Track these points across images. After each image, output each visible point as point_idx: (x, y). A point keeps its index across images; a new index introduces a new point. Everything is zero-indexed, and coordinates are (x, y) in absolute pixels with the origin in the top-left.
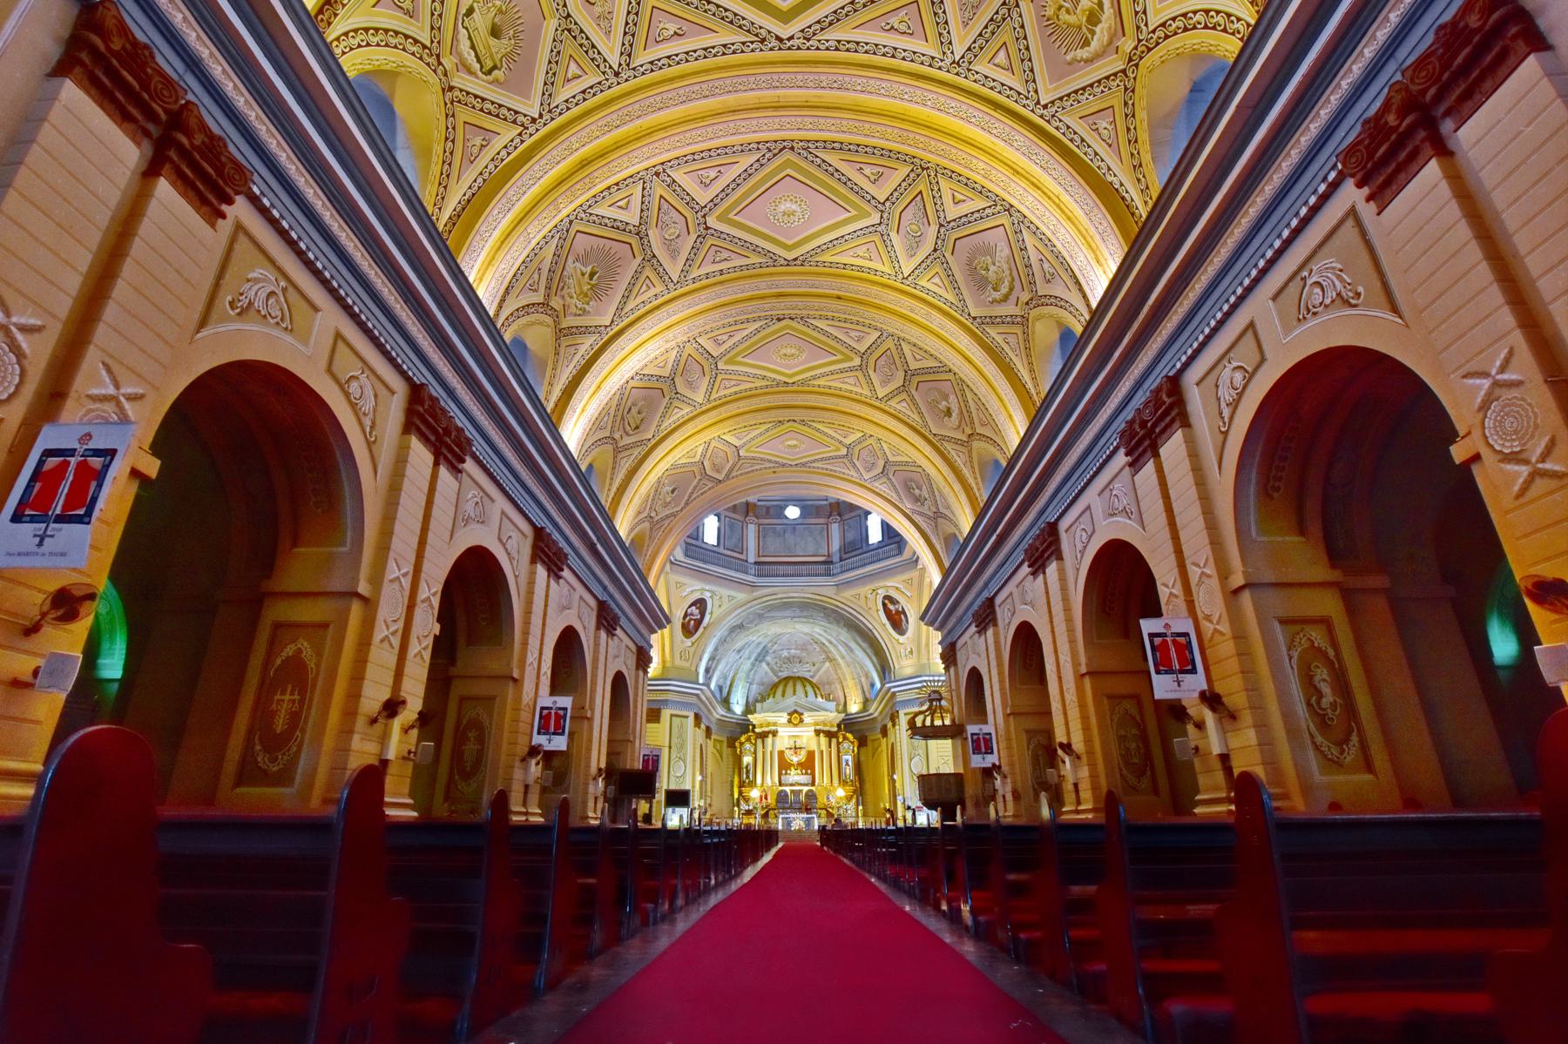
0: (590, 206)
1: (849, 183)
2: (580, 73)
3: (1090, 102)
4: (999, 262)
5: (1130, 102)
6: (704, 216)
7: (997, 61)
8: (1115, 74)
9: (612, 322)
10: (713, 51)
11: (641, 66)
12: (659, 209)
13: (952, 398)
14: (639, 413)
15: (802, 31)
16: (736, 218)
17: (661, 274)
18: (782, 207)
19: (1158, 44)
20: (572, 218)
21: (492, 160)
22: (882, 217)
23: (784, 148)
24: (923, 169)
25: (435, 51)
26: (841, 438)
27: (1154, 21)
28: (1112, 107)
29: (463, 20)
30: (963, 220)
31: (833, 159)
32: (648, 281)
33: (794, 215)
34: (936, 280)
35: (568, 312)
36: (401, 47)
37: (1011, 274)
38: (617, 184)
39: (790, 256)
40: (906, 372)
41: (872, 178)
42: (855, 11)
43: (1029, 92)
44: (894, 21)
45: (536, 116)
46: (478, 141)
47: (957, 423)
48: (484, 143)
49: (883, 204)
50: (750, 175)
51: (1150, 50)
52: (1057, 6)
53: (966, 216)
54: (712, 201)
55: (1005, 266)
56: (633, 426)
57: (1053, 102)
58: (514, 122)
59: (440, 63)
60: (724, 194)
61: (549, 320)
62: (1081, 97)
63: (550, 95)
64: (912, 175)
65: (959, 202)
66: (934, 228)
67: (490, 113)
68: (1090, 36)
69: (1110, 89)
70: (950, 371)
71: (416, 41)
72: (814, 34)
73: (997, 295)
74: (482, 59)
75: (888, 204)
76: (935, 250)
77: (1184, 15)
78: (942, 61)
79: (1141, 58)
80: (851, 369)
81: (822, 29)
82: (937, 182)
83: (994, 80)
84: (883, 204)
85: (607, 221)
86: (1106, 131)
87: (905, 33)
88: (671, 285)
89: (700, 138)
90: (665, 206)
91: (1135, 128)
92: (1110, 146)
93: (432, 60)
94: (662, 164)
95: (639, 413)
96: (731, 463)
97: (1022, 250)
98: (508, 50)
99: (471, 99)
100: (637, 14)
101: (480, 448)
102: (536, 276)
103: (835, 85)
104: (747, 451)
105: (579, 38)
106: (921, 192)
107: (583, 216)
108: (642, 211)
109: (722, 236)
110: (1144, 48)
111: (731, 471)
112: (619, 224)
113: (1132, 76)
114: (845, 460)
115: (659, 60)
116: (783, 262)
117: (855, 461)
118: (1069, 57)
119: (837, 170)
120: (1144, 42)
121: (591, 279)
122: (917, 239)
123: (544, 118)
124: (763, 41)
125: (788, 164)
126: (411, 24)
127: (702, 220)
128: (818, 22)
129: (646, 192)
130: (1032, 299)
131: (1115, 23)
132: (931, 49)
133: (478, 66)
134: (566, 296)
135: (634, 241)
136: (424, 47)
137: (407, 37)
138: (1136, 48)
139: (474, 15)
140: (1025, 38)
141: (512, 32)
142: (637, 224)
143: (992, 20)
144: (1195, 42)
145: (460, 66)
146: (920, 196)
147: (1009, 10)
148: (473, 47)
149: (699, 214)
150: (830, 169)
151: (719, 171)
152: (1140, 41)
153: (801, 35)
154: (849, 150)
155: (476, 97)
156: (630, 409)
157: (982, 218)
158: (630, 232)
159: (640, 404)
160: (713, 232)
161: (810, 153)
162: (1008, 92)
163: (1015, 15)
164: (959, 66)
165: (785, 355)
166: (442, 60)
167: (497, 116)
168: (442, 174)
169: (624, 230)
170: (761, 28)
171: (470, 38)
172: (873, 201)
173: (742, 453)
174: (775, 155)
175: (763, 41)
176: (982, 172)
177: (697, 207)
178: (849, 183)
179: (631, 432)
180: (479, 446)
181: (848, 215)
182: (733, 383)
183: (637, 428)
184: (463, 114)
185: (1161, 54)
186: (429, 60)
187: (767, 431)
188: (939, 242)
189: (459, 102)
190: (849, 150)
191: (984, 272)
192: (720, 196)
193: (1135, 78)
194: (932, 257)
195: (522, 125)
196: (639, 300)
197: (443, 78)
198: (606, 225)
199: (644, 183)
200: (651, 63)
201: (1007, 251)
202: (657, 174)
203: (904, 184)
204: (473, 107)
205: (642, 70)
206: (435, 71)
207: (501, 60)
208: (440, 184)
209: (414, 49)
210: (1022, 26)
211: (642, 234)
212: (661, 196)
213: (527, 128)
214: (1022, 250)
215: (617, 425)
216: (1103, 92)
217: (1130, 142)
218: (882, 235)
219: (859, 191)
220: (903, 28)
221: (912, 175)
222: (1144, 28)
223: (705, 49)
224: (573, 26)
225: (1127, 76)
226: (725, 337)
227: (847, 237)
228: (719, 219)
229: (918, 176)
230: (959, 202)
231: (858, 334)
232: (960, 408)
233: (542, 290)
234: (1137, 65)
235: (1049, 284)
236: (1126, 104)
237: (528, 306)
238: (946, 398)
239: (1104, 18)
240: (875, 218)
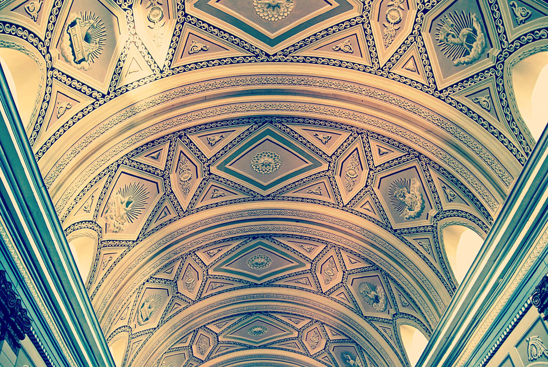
0: (133, 156)
1: (308, 144)
2: (138, 68)
3: (461, 92)
4: (412, 191)
5: (501, 84)
6: (209, 166)
7: (407, 66)
9: (138, 238)
10: (225, 61)
11: (178, 68)
12: (179, 160)
13: (379, 288)
14: (149, 308)
15: (283, 51)
16: (231, 167)
17: (175, 205)
18: (262, 161)
19: (516, 50)
20: (120, 162)
21: (72, 118)
22: (329, 166)
23: (266, 122)
24: (358, 134)
25: (47, 44)
26: (294, 325)
27: (511, 38)
28: (489, 88)
29: (68, 29)
30: (386, 165)
31: (298, 129)
32: (166, 210)
33: (270, 166)
34: (367, 206)
35: (108, 229)
36: (25, 38)
37: (422, 199)
38: (153, 142)
39: (265, 193)
40: (344, 272)
41: (324, 141)
42: (317, 40)
43: (430, 83)
44: (341, 45)
45: (106, 93)
46: (65, 105)
47: (383, 307)
48: (69, 107)
49: (331, 157)
50: (242, 139)
51: (510, 53)
52: (446, 34)
53: (388, 162)
54: (215, 155)
55: (417, 194)
56: (145, 318)
57: (446, 89)
58: (91, 95)
59: (48, 52)
60: (223, 151)
61: (95, 234)
62: (466, 84)
63: (117, 81)
64: (351, 138)
65: (384, 153)
66: (366, 171)
67: (75, 88)
68: (469, 49)
69: (485, 78)
70: (377, 269)
71: (36, 36)
72: (290, 53)
73: (412, 213)
74: (76, 53)
75: (334, 157)
76: (366, 186)
77: (533, 32)
78: (371, 68)
79: (505, 59)
80: (304, 272)
81: (295, 50)
82: (368, 142)
83: (406, 78)
84: (331, 157)
85: (143, 166)
86: (485, 103)
87: (348, 52)
88: (182, 213)
89: (212, 114)
90: (183, 158)
91: (506, 99)
92: (489, 111)
93: (44, 49)
94: (184, 130)
95: (149, 308)
96: (212, 346)
97: (429, 182)
98: (94, 50)
99: (64, 78)
100: (179, 36)
101: (35, 328)
102: (90, 201)
103: (302, 83)
104: (224, 337)
105: (140, 49)
106: (357, 149)
107: (127, 162)
108: (167, 161)
109: (220, 179)
110: (507, 53)
111: (211, 353)
112: (151, 169)
113: (500, 69)
114: (296, 341)
115: (190, 65)
116: (260, 197)
117: (304, 341)
118: (455, 62)
119: (300, 136)
120: (506, 50)
121: (127, 207)
122: (354, 180)
123: (110, 95)
124: (257, 56)
125: (268, 132)
126: (35, 26)
127: (207, 168)
128: (293, 46)
129: (171, 149)
130: (438, 214)
131: (486, 41)
132: (365, 61)
133: (73, 57)
134: (109, 217)
135: (160, 181)
136: (40, 40)
137: (30, 32)
138: (501, 53)
139: (76, 26)
140: (426, 53)
141: (98, 40)
142: (163, 170)
143: (404, 43)
144: (542, 46)
145: (61, 56)
146: (356, 151)
147: (415, 37)
148: (71, 46)
149: (206, 164)
150: (296, 135)
152: (503, 49)
153: (281, 53)
154: (309, 123)
155: (68, 76)
156: (144, 304)
157: (399, 163)
158: (158, 175)
159: (150, 302)
160: (214, 176)
161: (283, 125)
162: (416, 85)
163: (419, 40)
164: (383, 71)
165: (257, 263)
166: (49, 50)
167: (80, 90)
168: (37, 123)
169: (154, 173)
170: (256, 48)
171: (70, 40)
172: (323, 156)
173: (220, 339)
174: (259, 126)
175: (257, 56)
176: (400, 133)
177: (204, 159)
178: (308, 144)
179: (142, 323)
180: (36, 327)
181: (307, 165)
182: (218, 285)
183: (147, 319)
184: (57, 86)
185: (519, 55)
186: (41, 49)
187: (240, 321)
188: (369, 181)
189: (56, 78)
190: (309, 123)
191: (401, 199)
192: (221, 153)
193: (502, 70)
194: (364, 191)
195: (96, 98)
196: (159, 222)
197: (49, 62)
198: (142, 169)
199: (171, 142)
200: (185, 66)
201: (418, 184)
202: (180, 137)
203: (345, 144)
204: (65, 83)
205: (178, 70)
206: (44, 56)
208: (34, 129)
209: (34, 40)
210: (424, 46)
211: (165, 177)
212: (181, 152)
213: (98, 100)
214: (429, 182)
215: (133, 316)
216: (480, 80)
217: (503, 107)
218: (329, 178)
219: (316, 151)
220: (347, 49)
221: (351, 138)
222: (506, 42)
223: (220, 60)
224: (137, 40)
225: (496, 70)
226: (215, 251)
227: (305, 180)
228: (219, 168)
229: (355, 138)
230: (384, 153)
231: (309, 247)
232: (386, 295)
233: (93, 212)
234: (503, 63)
235: (451, 203)
236: (498, 85)
237: (81, 222)
238: (374, 288)
239: (477, 38)
240: (325, 167)
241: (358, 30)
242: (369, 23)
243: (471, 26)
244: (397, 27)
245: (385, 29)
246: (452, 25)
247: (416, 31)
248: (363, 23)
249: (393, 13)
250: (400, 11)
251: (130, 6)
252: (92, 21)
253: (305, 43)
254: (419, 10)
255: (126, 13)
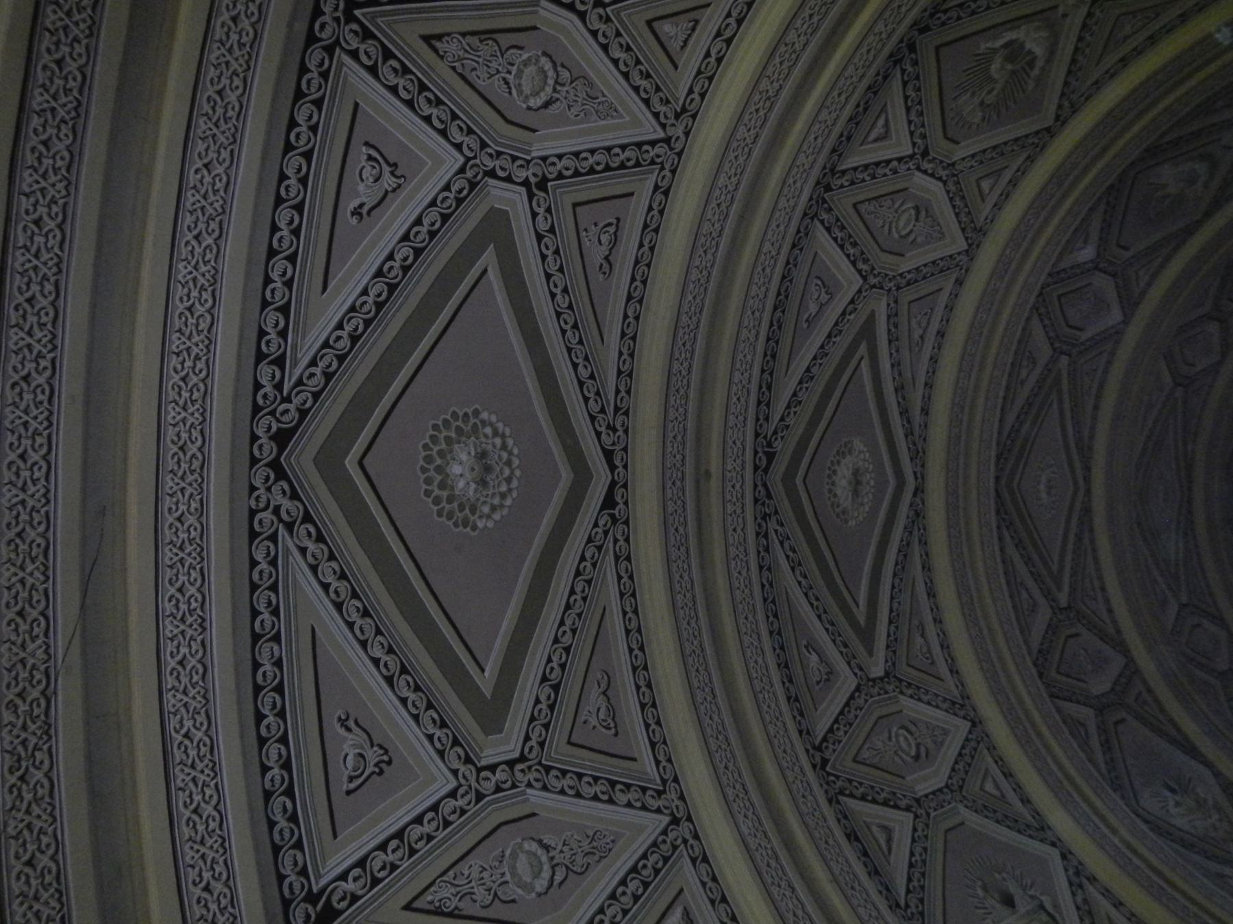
2: (990, 779)
8: (1089, 15)
15: (911, 459)
18: (1044, 495)
22: (1064, 353)
72: (914, 444)
76: (1114, 275)
81: (912, 434)
118: (1031, 85)
147: (954, 175)
151: (1021, 584)
164: (973, 244)
207: (1032, 897)
241: (907, 296)
242: (901, 275)
243: (994, 51)
244: (923, 214)
245: (919, 240)
246: (973, 94)
247: (943, 173)
248: (899, 288)
249: (902, 223)
250: (904, 208)
251: (917, 801)
252: (980, 892)
253: (905, 413)
254: (918, 169)
255: (933, 814)
